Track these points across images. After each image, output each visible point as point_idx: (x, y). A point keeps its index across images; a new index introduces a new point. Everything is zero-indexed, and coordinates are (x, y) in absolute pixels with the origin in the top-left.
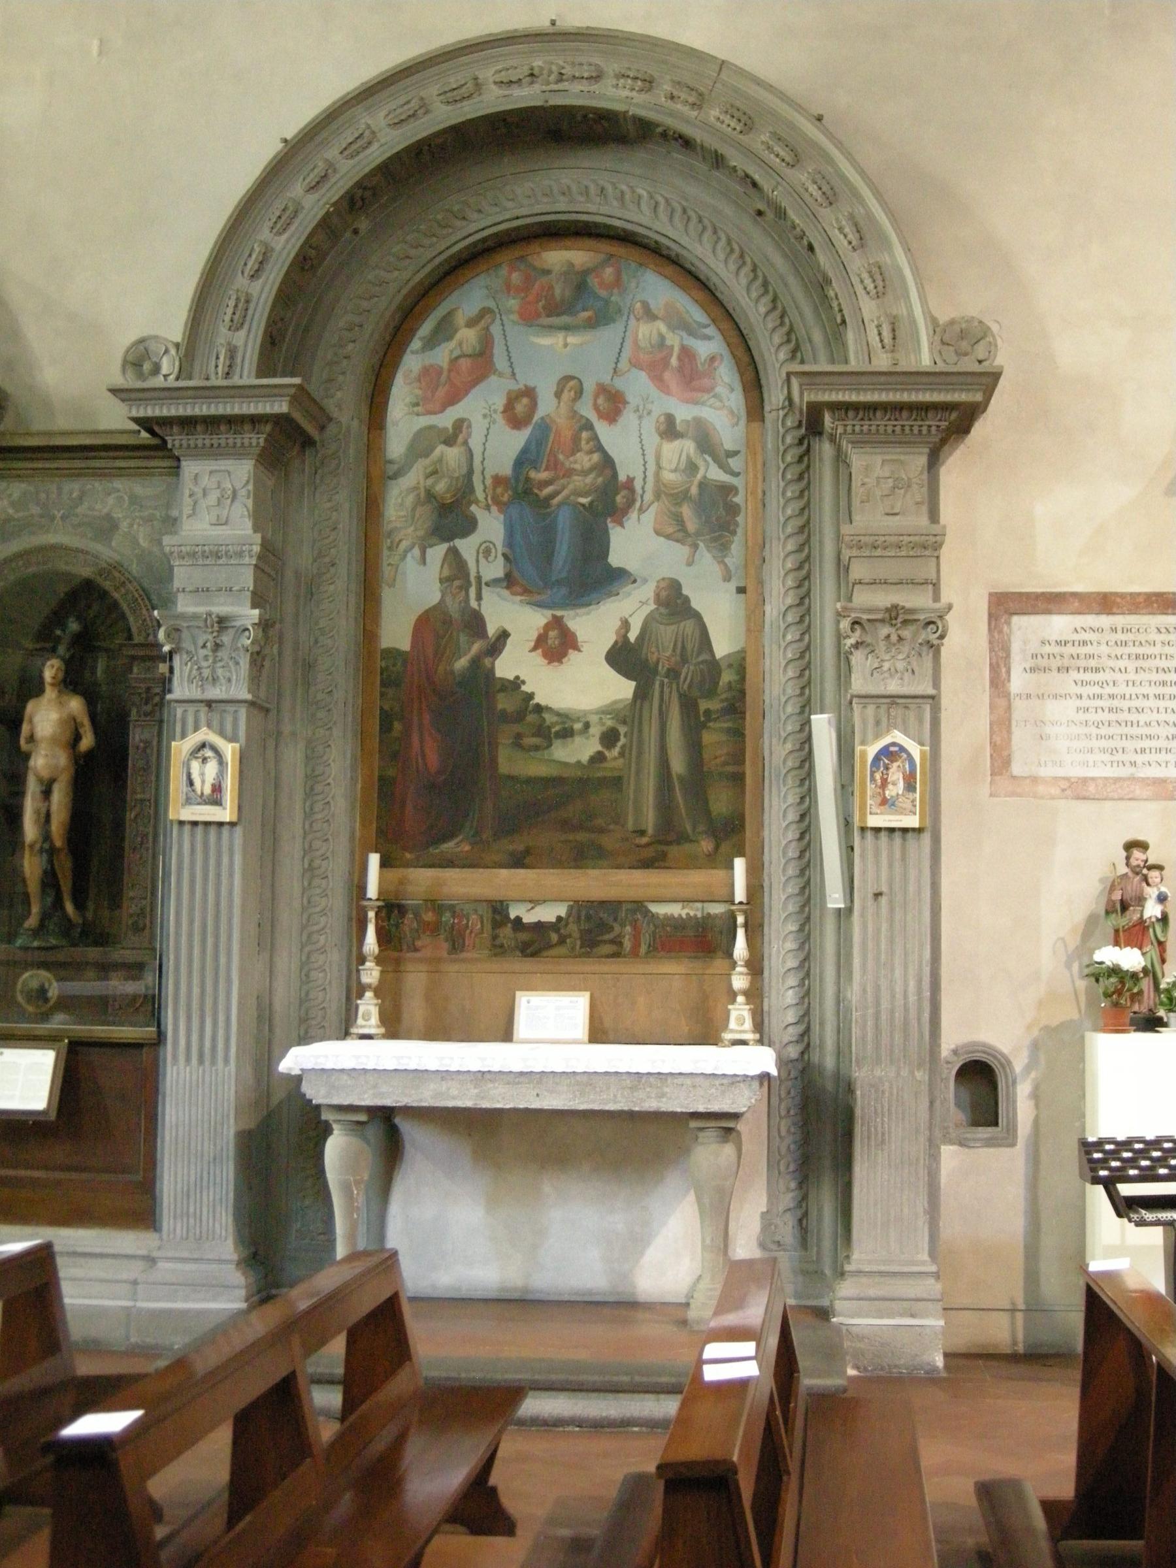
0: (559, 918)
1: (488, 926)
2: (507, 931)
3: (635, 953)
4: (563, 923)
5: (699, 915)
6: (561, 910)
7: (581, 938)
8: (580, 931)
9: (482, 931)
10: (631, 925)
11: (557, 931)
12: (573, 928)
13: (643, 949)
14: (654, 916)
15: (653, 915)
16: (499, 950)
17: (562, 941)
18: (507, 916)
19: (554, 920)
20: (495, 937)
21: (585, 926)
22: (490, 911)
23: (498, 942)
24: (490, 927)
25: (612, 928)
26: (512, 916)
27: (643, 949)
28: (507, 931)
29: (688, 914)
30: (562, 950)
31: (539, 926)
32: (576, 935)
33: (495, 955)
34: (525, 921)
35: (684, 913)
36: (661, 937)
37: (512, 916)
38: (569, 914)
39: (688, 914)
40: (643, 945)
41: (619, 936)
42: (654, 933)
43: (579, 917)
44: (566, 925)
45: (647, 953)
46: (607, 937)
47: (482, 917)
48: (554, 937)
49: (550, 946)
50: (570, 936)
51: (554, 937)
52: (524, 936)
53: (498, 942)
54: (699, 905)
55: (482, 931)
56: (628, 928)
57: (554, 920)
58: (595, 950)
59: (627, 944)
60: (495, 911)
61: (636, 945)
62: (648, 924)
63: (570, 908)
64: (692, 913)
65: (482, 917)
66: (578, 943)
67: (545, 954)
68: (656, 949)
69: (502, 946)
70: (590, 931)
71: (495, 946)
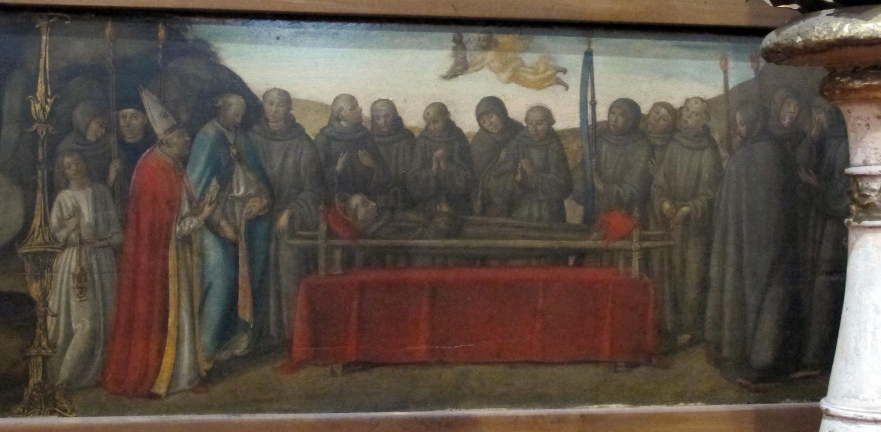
5: (566, 115)
10: (95, 174)
13: (182, 354)
14: (260, 117)
15: (254, 107)
27: (182, 354)
29: (492, 106)
35: (464, 99)
36: (308, 261)
39: (492, 106)
40: (179, 316)
42: (259, 227)
45: (205, 380)
54: (567, 53)
56: (77, 202)
62: (221, 172)
64: (519, 103)
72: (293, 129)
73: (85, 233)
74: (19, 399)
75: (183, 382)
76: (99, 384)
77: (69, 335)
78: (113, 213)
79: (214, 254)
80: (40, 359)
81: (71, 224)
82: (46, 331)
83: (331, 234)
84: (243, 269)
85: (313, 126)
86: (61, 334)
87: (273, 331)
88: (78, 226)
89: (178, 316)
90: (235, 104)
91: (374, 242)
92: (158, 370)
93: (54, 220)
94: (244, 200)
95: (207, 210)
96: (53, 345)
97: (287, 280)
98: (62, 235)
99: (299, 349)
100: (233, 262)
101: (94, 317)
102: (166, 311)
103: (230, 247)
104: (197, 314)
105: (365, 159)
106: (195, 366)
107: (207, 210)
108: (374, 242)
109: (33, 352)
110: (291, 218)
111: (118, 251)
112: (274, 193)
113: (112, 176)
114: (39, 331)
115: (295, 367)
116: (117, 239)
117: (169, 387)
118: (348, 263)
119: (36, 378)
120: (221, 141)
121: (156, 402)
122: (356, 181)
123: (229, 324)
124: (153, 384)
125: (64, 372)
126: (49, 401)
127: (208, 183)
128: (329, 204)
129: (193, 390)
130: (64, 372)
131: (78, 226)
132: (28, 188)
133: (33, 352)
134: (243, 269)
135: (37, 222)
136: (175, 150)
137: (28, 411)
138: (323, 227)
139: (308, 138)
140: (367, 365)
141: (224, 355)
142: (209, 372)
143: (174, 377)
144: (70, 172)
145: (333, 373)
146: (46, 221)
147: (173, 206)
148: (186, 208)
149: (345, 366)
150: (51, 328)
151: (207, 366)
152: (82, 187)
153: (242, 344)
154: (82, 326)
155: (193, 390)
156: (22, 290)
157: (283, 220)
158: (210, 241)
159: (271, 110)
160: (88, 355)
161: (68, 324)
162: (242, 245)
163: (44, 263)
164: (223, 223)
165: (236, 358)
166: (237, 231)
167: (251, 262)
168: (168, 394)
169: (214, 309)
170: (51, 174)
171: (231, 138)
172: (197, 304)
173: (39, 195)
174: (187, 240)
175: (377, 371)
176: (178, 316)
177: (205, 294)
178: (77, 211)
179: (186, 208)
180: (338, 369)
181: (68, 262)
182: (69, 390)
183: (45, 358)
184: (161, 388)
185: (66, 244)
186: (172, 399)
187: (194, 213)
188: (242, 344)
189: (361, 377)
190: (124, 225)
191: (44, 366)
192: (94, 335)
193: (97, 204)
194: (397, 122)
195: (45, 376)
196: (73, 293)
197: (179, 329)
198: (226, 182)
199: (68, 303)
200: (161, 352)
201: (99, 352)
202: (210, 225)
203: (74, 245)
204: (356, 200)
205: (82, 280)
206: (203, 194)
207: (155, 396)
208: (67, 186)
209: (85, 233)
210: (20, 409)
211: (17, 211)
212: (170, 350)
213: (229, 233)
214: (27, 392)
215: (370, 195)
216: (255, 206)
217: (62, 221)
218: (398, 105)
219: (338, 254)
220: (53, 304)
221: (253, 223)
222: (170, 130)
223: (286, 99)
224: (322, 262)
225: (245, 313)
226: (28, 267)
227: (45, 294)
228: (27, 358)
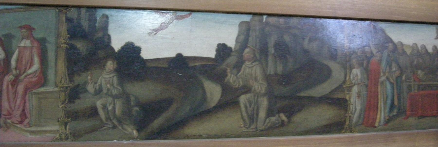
0: (223, 50)
1: (58, 69)
2: (106, 76)
3: (368, 123)
4: (232, 60)
6: (226, 32)
7: (270, 94)
8: (268, 78)
9: (43, 79)
11: (218, 77)
12: (252, 71)
13: (382, 115)
16: (87, 124)
17: (229, 102)
18: (105, 42)
19: (210, 53)
20: (74, 94)
21: (275, 67)
22: (64, 29)
23: (83, 103)
24: (62, 66)
25: (326, 74)
26: (117, 44)
27: (382, 115)
28: (106, 76)
30: (230, 120)
31: (179, 66)
32: (260, 86)
33: (76, 136)
34: (146, 55)
37: (117, 44)
38: (244, 41)
40: (381, 104)
41: (340, 88)
43: (264, 50)
44: (238, 67)
45: (387, 122)
46: (319, 91)
47: (42, 42)
48: (214, 92)
49: (203, 113)
50: (246, 89)
51: (214, 92)
52: (144, 91)
53: (83, 103)
55: (43, 79)
57: (212, 54)
58: (298, 118)
59: (356, 105)
60: (76, 32)
61: (371, 107)
62: (389, 64)
63: (245, 31)
65: (42, 43)
66: (264, 103)
67: (193, 128)
68: (402, 112)
69: (93, 112)
70: (286, 79)
71: (74, 116)
72: (404, 52)
73: (359, 81)
74: (343, 129)
75: (382, 123)
76: (362, 124)
77: (356, 110)
78: (365, 75)
79: (389, 87)
80: (348, 117)
81: (356, 79)
82: (350, 109)
83: (415, 81)
84: (395, 91)
85: (408, 51)
86: (354, 110)
87: (402, 108)
88: (357, 79)
89: (381, 104)
90: (391, 46)
91: (424, 83)
92: (376, 119)
93: (352, 77)
94: (395, 71)
95: (387, 75)
96: (352, 113)
97: (405, 94)
98: (353, 82)
99: (408, 113)
100: (393, 89)
101: (361, 104)
102: (378, 102)
103: (392, 84)
104: (385, 103)
105: (421, 61)
106: (385, 118)
107: (387, 75)
108: (424, 83)
109: (347, 115)
110: (406, 77)
111: (367, 86)
112: (402, 70)
113: (364, 65)
114: (348, 109)
115: (407, 117)
116: (366, 83)
117: (379, 124)
118: (418, 89)
119: (347, 122)
120: (389, 56)
121: (375, 128)
122: (418, 67)
123: (392, 106)
124: (375, 123)
125: (354, 120)
126: (350, 130)
127: (386, 67)
128: (414, 73)
129: (384, 125)
130: (354, 120)
131: (357, 79)
132: (345, 68)
133: (347, 115)
134: (395, 91)
135: (347, 78)
136: (378, 58)
137: (345, 132)
138: (413, 79)
139: (407, 55)
140: (423, 117)
141: (391, 115)
142: (388, 119)
143: (380, 122)
144: (355, 64)
145: (415, 120)
146: (350, 78)
147: (379, 73)
148: (382, 74)
149: (418, 117)
150: (351, 108)
151: (387, 118)
152: (358, 68)
153: (395, 112)
154: (359, 108)
155: (384, 125)
156: (344, 97)
157: (404, 77)
158: (388, 83)
159: (399, 47)
160: (360, 116)
161: (355, 107)
162: (395, 85)
163: (350, 89)
164: (390, 78)
165: (394, 115)
166: (394, 81)
167: (397, 89)
168: (379, 126)
169: (389, 102)
170: (350, 65)
171: (391, 55)
172: (385, 100)
173: (348, 71)
174: (382, 83)
175: (425, 118)
176: (381, 104)
177: (387, 98)
178: (357, 75)
179: (382, 74)
180: (416, 118)
181: (355, 89)
182: (356, 125)
183: (350, 116)
184: (377, 125)
185: (354, 85)
186: (379, 128)
187: (384, 75)
188: (395, 112)
189: (422, 120)
190: (368, 79)
191: (350, 119)
192: (361, 110)
193: (362, 73)
194: (426, 50)
195: (350, 122)
196: (356, 98)
197: (381, 108)
198: (390, 67)
199: (355, 101)
200: (377, 114)
201: (362, 114)
202: (388, 78)
203: (356, 84)
204: (419, 72)
205: (359, 95)
206: (385, 70)
207: (375, 127)
208: (354, 68)
209: (359, 81)
210: (343, 131)
211: (343, 75)
212: (379, 113)
213: (392, 81)
214: (345, 126)
215: (423, 70)
216: (398, 73)
217: (354, 77)
218: (426, 46)
219: (416, 86)
220: (352, 101)
221: (397, 78)
222: (377, 53)
223: (402, 44)
224: (413, 89)
225: (396, 103)
226: (346, 91)
227: (350, 98)
228: (346, 116)
